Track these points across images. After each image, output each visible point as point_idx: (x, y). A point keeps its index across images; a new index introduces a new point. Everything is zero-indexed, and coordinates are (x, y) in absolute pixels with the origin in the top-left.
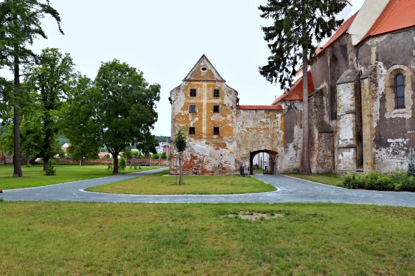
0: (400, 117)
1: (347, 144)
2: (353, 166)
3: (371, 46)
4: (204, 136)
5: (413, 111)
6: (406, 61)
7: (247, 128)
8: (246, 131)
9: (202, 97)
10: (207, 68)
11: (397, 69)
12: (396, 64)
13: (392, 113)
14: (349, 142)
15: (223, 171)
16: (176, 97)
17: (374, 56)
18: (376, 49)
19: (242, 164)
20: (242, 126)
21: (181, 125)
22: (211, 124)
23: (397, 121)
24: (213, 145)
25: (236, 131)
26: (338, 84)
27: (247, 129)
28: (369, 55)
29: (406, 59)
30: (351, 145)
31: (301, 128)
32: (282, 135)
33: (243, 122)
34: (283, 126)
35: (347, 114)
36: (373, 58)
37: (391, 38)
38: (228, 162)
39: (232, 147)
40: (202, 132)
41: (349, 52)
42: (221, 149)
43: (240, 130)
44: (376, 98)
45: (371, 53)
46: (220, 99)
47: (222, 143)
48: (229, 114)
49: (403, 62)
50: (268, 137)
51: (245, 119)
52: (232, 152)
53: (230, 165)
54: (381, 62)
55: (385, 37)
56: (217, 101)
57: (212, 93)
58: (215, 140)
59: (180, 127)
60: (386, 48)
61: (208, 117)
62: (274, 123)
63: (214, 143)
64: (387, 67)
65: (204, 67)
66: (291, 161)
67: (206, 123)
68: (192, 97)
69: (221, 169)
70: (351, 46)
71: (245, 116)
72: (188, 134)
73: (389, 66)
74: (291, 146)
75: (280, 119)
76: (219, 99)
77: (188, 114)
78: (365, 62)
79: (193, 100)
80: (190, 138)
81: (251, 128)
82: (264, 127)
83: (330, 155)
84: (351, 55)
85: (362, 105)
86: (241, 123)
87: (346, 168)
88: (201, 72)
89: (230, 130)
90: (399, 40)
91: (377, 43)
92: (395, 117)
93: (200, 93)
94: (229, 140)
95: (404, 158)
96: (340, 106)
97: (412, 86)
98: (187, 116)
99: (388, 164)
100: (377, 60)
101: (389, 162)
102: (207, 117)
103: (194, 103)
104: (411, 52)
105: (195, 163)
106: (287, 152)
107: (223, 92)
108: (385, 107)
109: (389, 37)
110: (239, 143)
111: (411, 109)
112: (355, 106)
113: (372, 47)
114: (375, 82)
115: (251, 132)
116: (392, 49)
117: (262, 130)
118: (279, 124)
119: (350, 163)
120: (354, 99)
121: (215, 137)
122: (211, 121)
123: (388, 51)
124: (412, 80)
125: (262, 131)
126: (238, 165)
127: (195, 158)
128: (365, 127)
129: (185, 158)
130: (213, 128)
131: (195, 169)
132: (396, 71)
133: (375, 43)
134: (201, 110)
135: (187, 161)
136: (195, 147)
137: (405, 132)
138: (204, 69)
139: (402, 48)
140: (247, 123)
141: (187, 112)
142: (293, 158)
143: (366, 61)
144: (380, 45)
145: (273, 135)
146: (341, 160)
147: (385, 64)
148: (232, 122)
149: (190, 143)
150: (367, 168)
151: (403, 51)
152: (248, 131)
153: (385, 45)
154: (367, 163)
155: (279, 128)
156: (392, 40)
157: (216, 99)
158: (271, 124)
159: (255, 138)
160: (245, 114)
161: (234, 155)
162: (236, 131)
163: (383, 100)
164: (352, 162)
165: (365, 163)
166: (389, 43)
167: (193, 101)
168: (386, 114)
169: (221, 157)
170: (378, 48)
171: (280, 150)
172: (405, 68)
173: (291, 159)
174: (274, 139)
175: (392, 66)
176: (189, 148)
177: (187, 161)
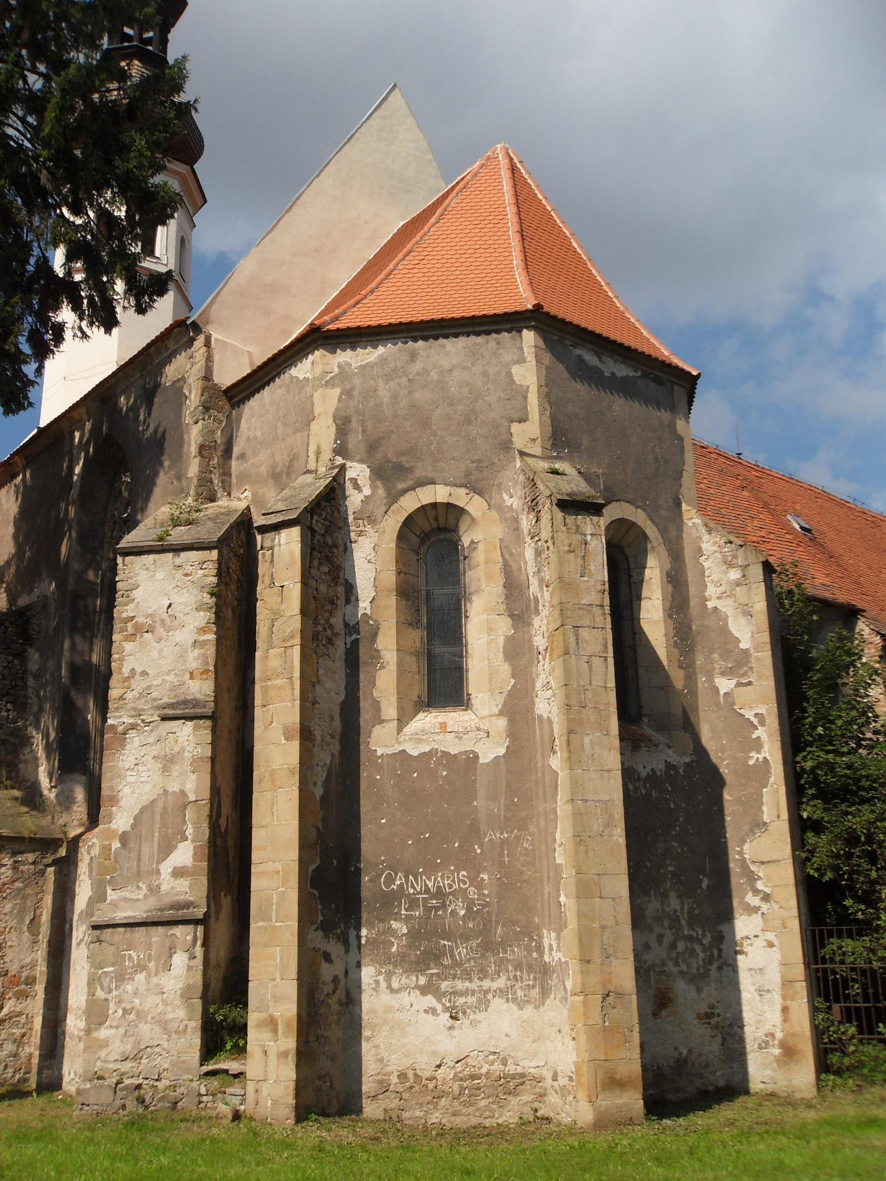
0: (446, 754)
1: (152, 903)
5: (512, 722)
6: (479, 469)
11: (434, 505)
12: (433, 482)
14: (164, 888)
18: (340, 399)
26: (127, 553)
28: (297, 431)
29: (479, 461)
35: (164, 719)
37: (413, 356)
44: (330, 642)
49: (467, 474)
54: (361, 461)
60: (386, 400)
64: (389, 492)
73: (400, 486)
78: (274, 465)
85: (258, 674)
91: (344, 373)
92: (427, 749)
95: (467, 984)
96: (126, 671)
97: (507, 597)
99: (385, 1022)
100: (341, 450)
104: (504, 430)
111: (501, 713)
112: (212, 675)
114: (328, 559)
116: (413, 406)
119: (164, 1025)
120: (211, 637)
123: (395, 416)
128: (268, 795)
132: (431, 514)
133: (336, 371)
137: (473, 833)
139: (460, 408)
143: (281, 459)
144: (357, 381)
146: (112, 1007)
147: (379, 474)
150: (272, 1055)
151: (469, 421)
153: (381, 383)
156: (418, 366)
165: (258, 1026)
170: (348, 393)
172: (475, 505)
175: (413, 488)
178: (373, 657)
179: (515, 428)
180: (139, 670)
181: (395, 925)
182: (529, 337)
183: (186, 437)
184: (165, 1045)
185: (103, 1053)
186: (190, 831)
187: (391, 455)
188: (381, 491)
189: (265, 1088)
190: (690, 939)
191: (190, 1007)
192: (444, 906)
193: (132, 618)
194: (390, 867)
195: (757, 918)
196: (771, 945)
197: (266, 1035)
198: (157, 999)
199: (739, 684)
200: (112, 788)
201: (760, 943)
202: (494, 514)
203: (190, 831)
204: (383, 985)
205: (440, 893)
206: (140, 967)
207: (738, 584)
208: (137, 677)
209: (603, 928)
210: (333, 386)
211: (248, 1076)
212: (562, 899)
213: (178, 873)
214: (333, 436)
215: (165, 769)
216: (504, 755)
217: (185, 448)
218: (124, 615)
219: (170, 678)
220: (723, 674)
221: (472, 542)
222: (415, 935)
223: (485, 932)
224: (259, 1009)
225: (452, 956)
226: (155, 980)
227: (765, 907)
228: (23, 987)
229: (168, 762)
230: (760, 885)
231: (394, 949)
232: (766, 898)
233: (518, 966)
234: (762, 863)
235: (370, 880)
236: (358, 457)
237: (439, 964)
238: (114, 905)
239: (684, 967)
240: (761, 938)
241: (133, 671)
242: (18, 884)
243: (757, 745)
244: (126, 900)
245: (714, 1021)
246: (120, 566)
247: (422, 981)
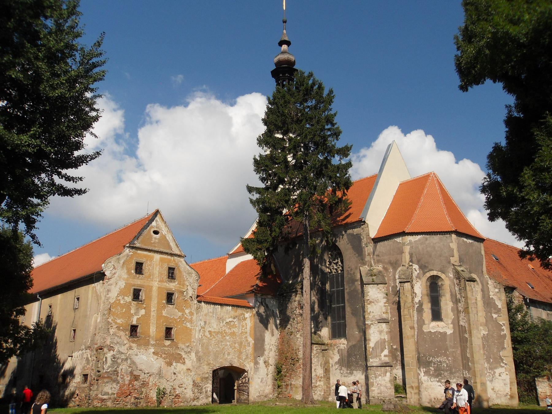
1: (380, 362)
2: (390, 391)
3: (404, 244)
4: (152, 342)
7: (209, 331)
8: (209, 336)
9: (152, 277)
10: (160, 231)
12: (433, 270)
13: (433, 327)
14: (383, 359)
15: (177, 400)
16: (114, 271)
17: (407, 257)
18: (410, 249)
19: (202, 388)
20: (204, 328)
21: (119, 321)
22: (163, 322)
23: (437, 336)
24: (163, 356)
25: (195, 334)
27: (210, 332)
29: (443, 266)
30: (386, 363)
31: (273, 335)
32: (251, 344)
33: (205, 322)
34: (253, 332)
36: (405, 259)
37: (426, 239)
38: (183, 386)
39: (191, 360)
40: (149, 333)
41: (366, 244)
42: (174, 364)
43: (201, 334)
45: (402, 252)
46: (177, 283)
47: (176, 353)
48: (187, 308)
49: (441, 269)
50: (235, 348)
51: (208, 318)
52: (189, 369)
53: (185, 391)
54: (416, 264)
55: (419, 237)
56: (172, 286)
57: (166, 273)
58: (166, 349)
59: (116, 323)
61: (160, 309)
62: (243, 326)
63: (165, 354)
64: (423, 272)
65: (156, 229)
66: (261, 384)
67: (155, 320)
68: (138, 275)
69: (173, 397)
70: (369, 238)
71: (208, 312)
72: (127, 337)
73: (426, 271)
74: (261, 361)
75: (249, 321)
76: (174, 282)
77: (130, 303)
79: (139, 281)
80: (132, 344)
81: (214, 332)
82: (230, 331)
83: (322, 376)
84: (369, 249)
86: (202, 324)
87: (381, 394)
88: (151, 236)
89: (188, 332)
90: (435, 244)
91: (411, 242)
92: (435, 331)
93: (149, 269)
94: (186, 349)
96: (369, 312)
97: (451, 297)
98: (128, 306)
100: (411, 261)
101: (431, 385)
102: (157, 311)
103: (140, 286)
105: (136, 387)
106: (256, 369)
107: (180, 272)
108: (423, 318)
109: (424, 237)
110: (199, 355)
111: (451, 323)
113: (404, 245)
115: (215, 337)
117: (228, 336)
118: (248, 327)
119: (386, 387)
121: (168, 343)
122: (162, 316)
124: (450, 290)
125: (228, 338)
126: (196, 390)
127: (136, 378)
129: (122, 378)
130: (165, 329)
131: (136, 398)
134: (149, 297)
135: (124, 385)
136: (137, 359)
137: (446, 349)
138: (156, 232)
140: (209, 323)
141: (129, 299)
142: (264, 380)
144: (414, 245)
145: (241, 344)
146: (375, 383)
147: (421, 267)
148: (191, 321)
149: (131, 352)
151: (441, 256)
152: (211, 336)
154: (412, 387)
155: (248, 334)
156: (428, 242)
157: (171, 282)
158: (239, 327)
159: (219, 347)
160: (208, 309)
161: (193, 373)
162: (197, 335)
163: (420, 310)
164: (389, 385)
165: (409, 387)
166: (425, 245)
167: (138, 281)
168: (424, 326)
169: (174, 377)
170: (412, 247)
171: (248, 366)
172: (443, 276)
173: (261, 382)
174: (242, 349)
175: (428, 271)
176: (129, 361)
177: (124, 385)
178: (422, 310)
179: (451, 258)
180: (371, 311)
181: (431, 368)
182: (454, 236)
183: (364, 250)
184: (387, 391)
185: (374, 392)
186: (387, 347)
187: (423, 263)
188: (421, 272)
189: (411, 400)
190: (489, 373)
191: (391, 384)
192: (441, 364)
193: (369, 300)
194: (429, 356)
195: (504, 369)
196: (507, 374)
197: (411, 390)
198: (384, 382)
199: (498, 316)
200: (369, 337)
201: (505, 374)
202: (447, 278)
203: (387, 347)
204: (429, 380)
205: (440, 362)
206: (380, 375)
207: (498, 292)
208: (371, 313)
209: (480, 370)
210: (408, 245)
211: (407, 397)
212: (470, 364)
213: (385, 356)
214: (409, 258)
215: (380, 334)
216: (453, 333)
217: (364, 253)
218: (367, 299)
219: (379, 313)
220: (494, 313)
221: (442, 284)
222: (435, 370)
223: (450, 370)
224: (408, 384)
225: (444, 375)
226: (383, 378)
227: (505, 366)
228: (320, 379)
229: (381, 332)
230: (504, 361)
231: (431, 373)
232: (506, 364)
233: (458, 377)
234: (505, 357)
235: (425, 358)
236: (415, 263)
237: (441, 376)
238: (372, 362)
239: (489, 379)
240: (505, 373)
241: (370, 311)
242: (317, 355)
243: (503, 330)
244: (374, 361)
245: (494, 390)
246: (365, 287)
247: (438, 380)
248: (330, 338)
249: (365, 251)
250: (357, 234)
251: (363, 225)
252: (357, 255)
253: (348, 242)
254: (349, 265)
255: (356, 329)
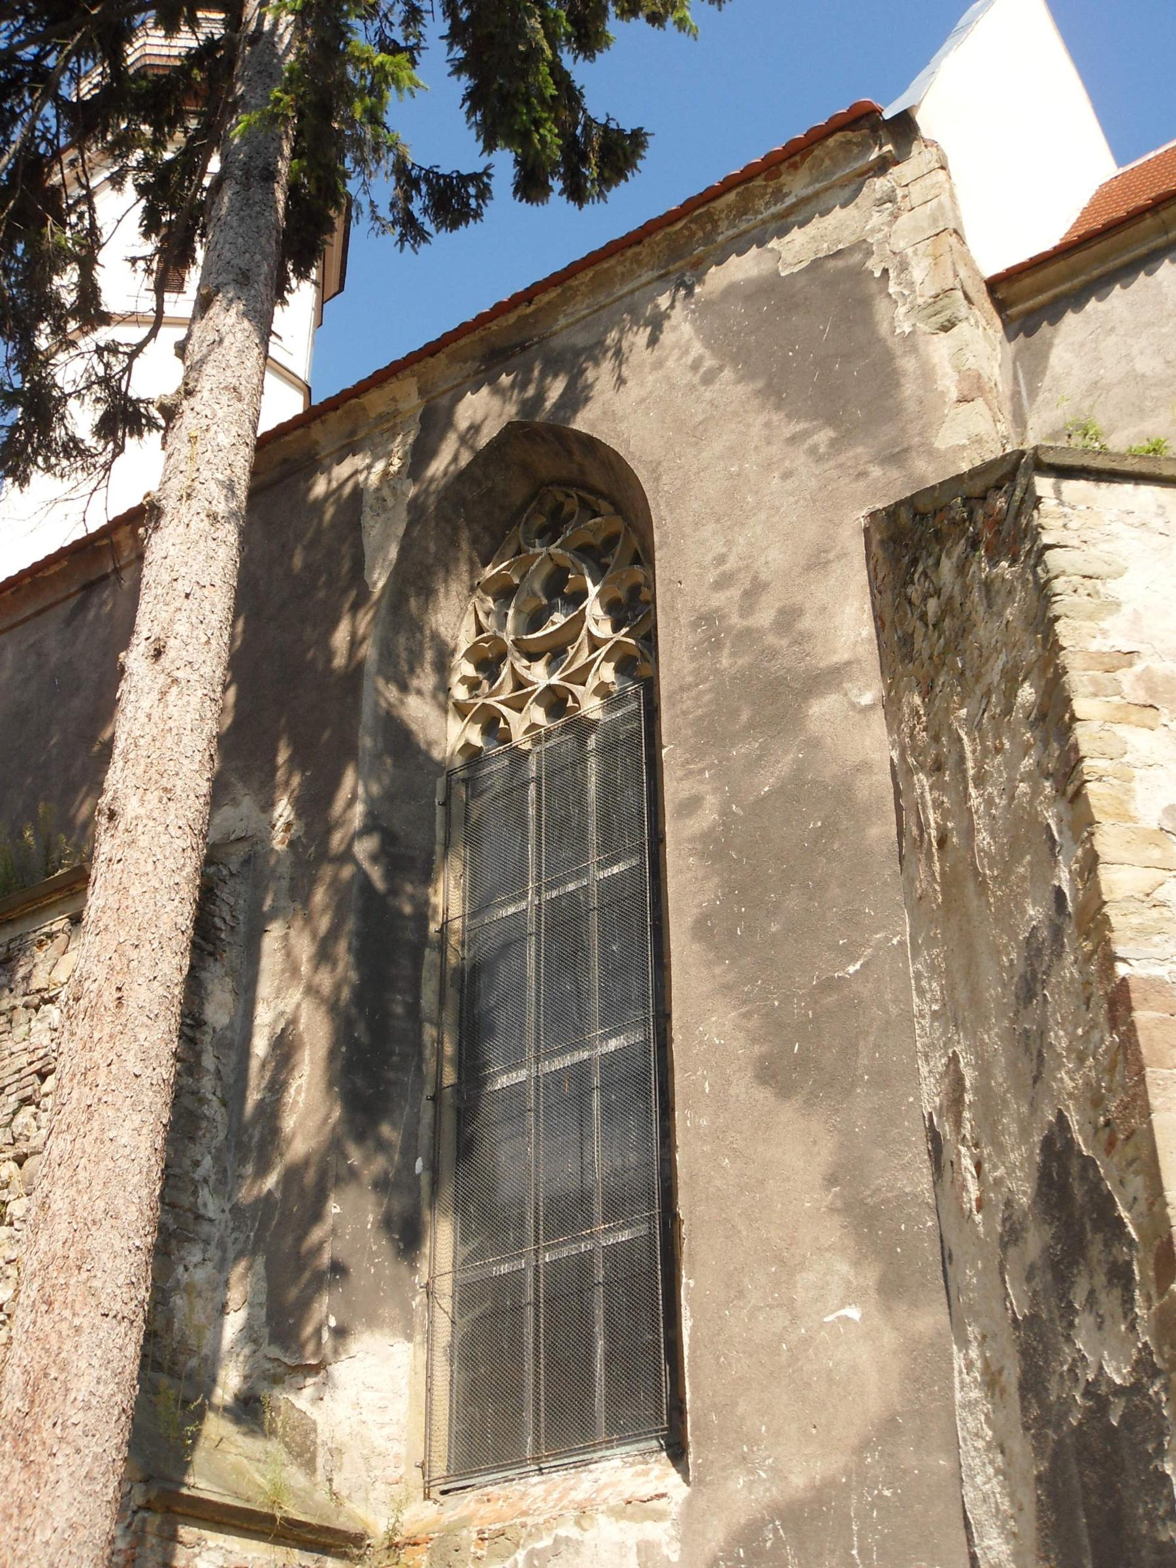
183: (908, 364)
217: (909, 388)
246: (1049, 504)
248: (440, 1468)
249: (927, 375)
250: (816, 264)
251: (883, 166)
252: (823, 437)
253: (709, 362)
254: (721, 559)
255: (843, 1267)
